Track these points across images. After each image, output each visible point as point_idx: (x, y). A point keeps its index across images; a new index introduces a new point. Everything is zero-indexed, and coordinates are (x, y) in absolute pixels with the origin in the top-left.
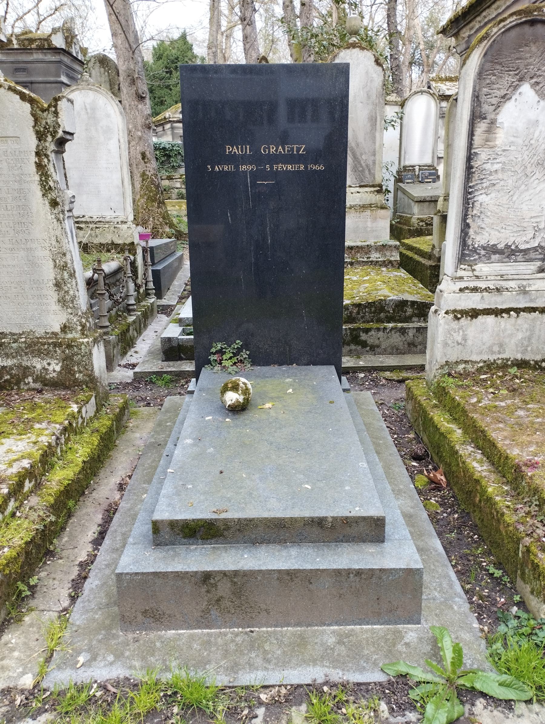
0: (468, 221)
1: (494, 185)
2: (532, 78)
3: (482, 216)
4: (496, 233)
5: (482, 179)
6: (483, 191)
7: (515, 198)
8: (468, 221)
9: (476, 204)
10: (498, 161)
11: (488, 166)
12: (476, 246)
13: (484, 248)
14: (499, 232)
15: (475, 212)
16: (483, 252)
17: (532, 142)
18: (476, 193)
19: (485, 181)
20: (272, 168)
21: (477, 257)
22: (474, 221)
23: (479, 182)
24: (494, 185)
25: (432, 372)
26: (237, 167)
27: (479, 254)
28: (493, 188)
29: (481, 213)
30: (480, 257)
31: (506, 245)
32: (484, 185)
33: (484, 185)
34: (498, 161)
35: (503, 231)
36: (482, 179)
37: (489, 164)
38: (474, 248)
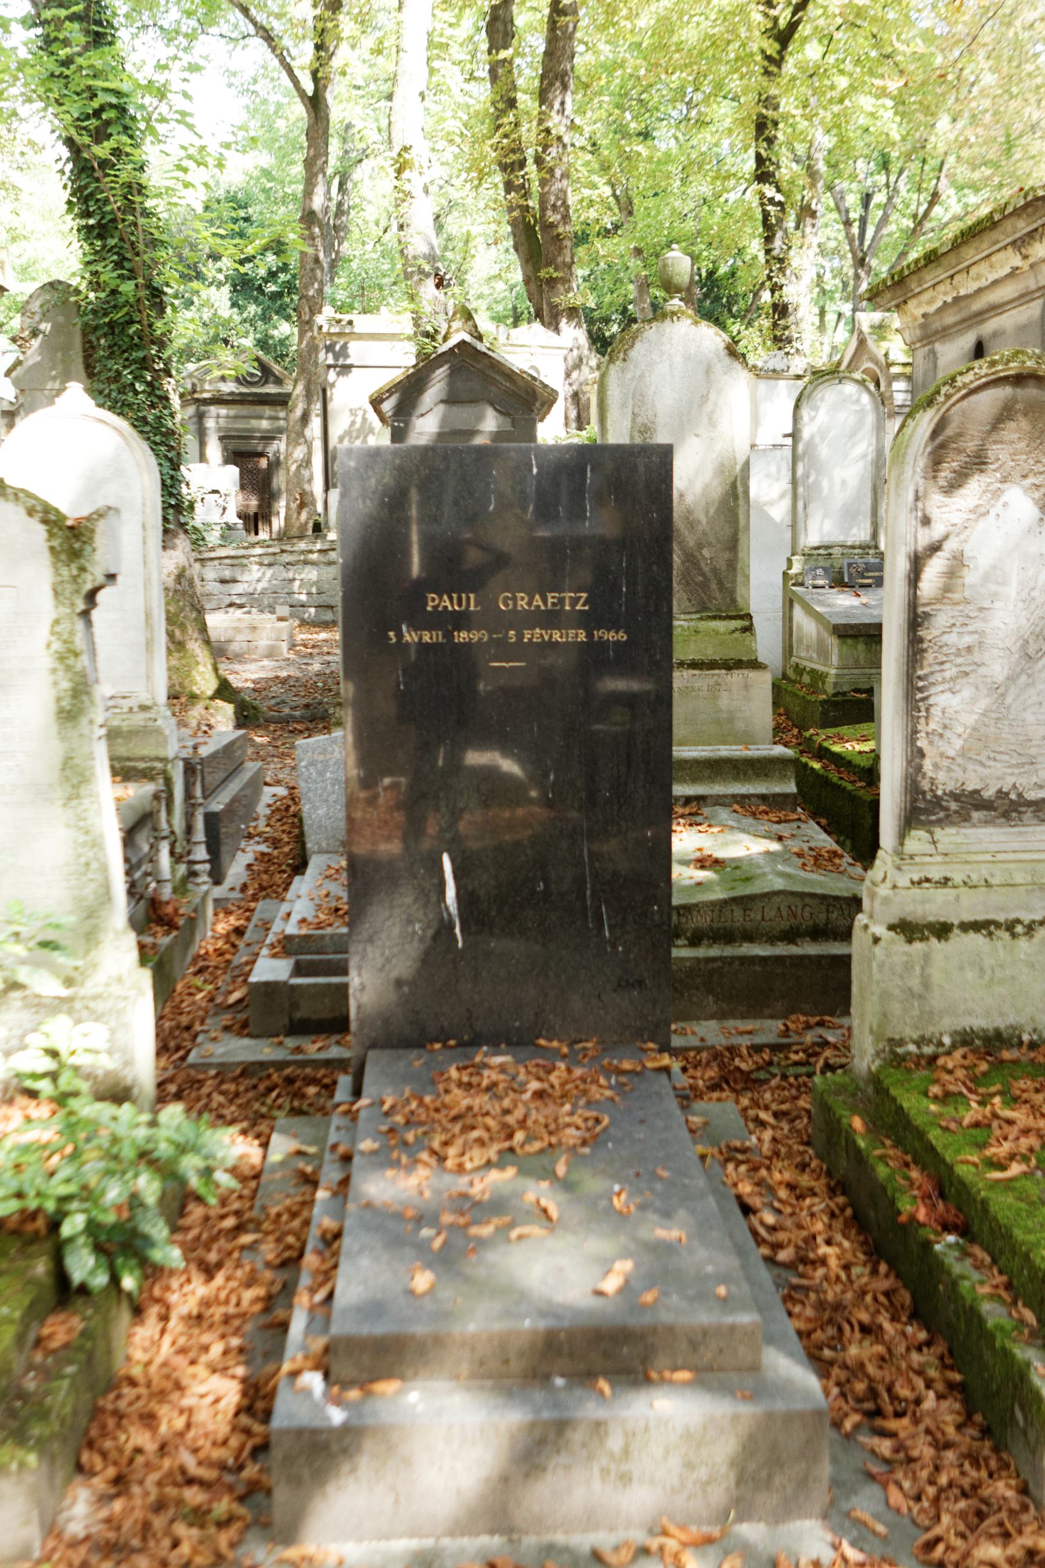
0: (919, 744)
1: (967, 674)
2: (1024, 477)
3: (948, 734)
4: (978, 768)
5: (942, 663)
6: (947, 686)
7: (1009, 700)
8: (919, 744)
9: (932, 710)
10: (970, 628)
11: (951, 639)
12: (940, 793)
13: (955, 797)
14: (983, 765)
15: (932, 726)
16: (954, 806)
17: (1034, 594)
18: (933, 690)
19: (947, 666)
20: (520, 636)
21: (942, 814)
22: (931, 743)
23: (937, 668)
24: (967, 674)
25: (865, 1057)
26: (449, 635)
27: (946, 809)
28: (964, 681)
29: (945, 727)
30: (948, 816)
31: (1000, 791)
32: (947, 675)
33: (947, 675)
34: (970, 628)
35: (992, 763)
36: (942, 663)
37: (954, 635)
38: (935, 796)
